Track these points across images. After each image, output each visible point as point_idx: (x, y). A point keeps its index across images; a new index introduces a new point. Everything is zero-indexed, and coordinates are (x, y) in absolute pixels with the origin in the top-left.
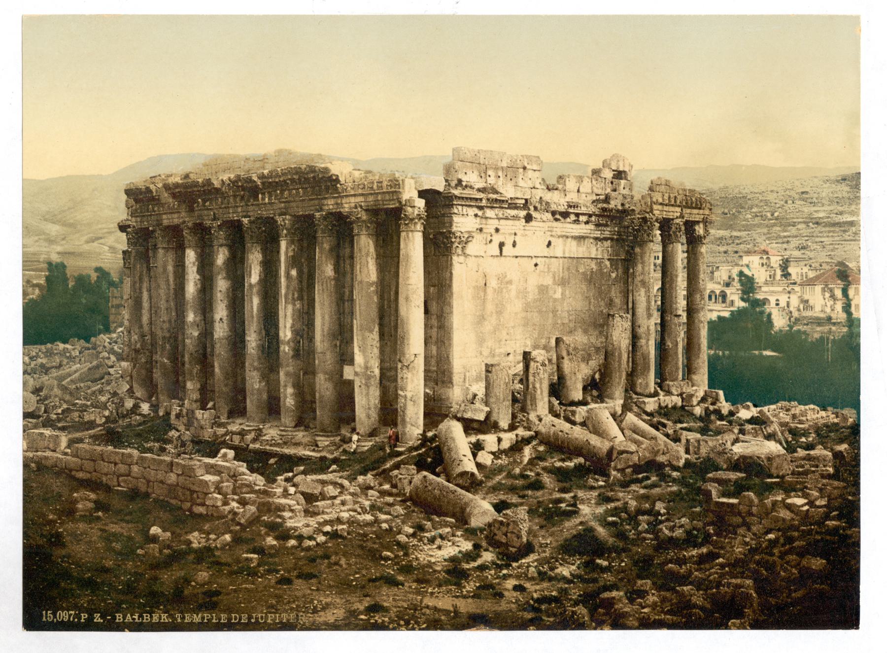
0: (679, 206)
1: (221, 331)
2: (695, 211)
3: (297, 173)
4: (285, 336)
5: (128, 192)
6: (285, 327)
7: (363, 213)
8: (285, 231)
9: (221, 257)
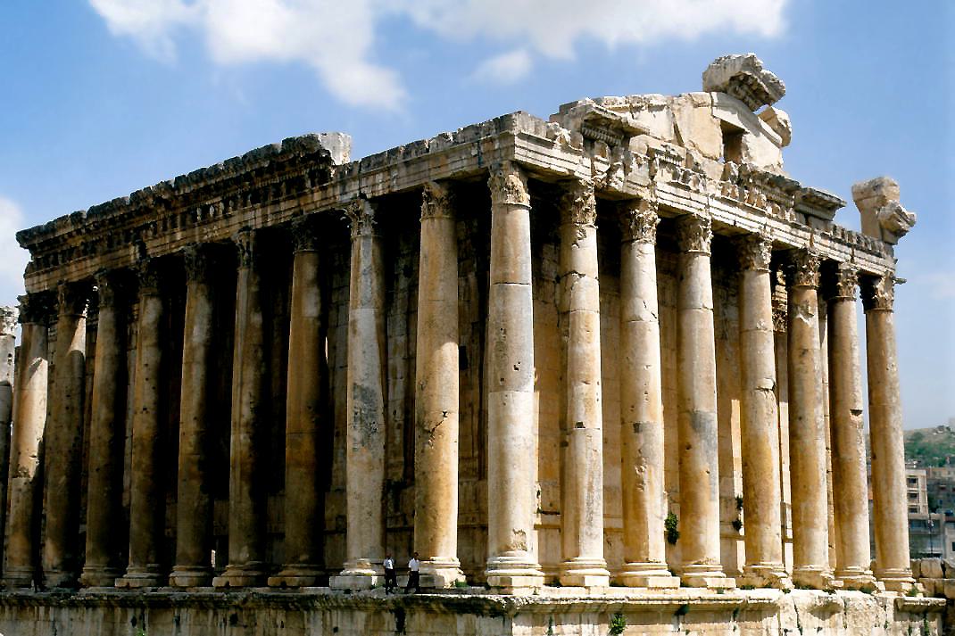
0: (849, 246)
1: (140, 425)
2: (874, 258)
3: (267, 157)
4: (241, 416)
5: (25, 238)
6: (241, 402)
7: (368, 205)
8: (246, 254)
9: (149, 312)
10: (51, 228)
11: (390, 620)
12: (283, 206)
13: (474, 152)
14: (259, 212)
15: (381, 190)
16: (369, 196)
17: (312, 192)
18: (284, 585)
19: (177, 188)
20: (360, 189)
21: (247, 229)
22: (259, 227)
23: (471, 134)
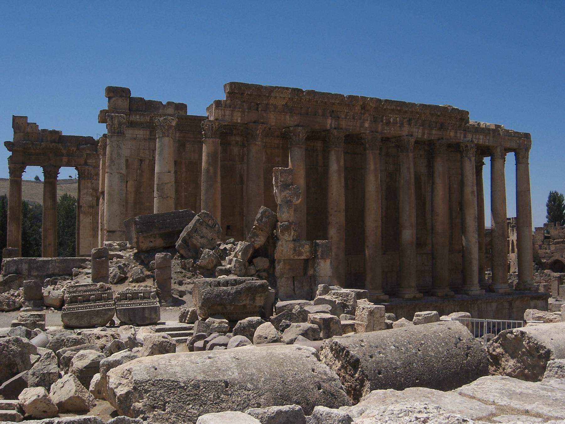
10: (272, 89)
11: (506, 305)
12: (434, 132)
13: (518, 142)
14: (420, 131)
15: (481, 142)
16: (476, 142)
17: (450, 131)
18: (446, 295)
19: (383, 105)
20: (472, 139)
21: (412, 136)
22: (420, 136)
23: (517, 135)
